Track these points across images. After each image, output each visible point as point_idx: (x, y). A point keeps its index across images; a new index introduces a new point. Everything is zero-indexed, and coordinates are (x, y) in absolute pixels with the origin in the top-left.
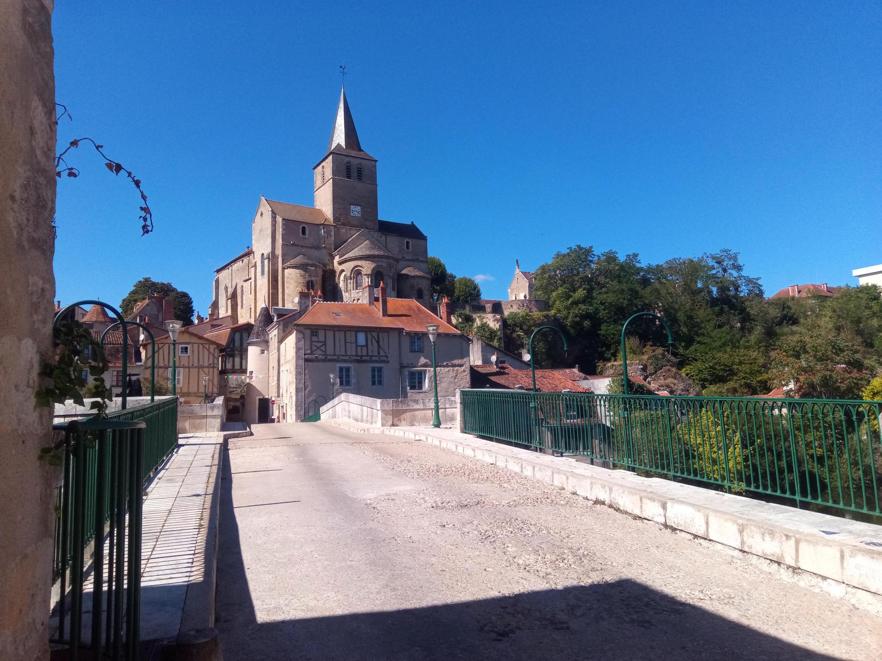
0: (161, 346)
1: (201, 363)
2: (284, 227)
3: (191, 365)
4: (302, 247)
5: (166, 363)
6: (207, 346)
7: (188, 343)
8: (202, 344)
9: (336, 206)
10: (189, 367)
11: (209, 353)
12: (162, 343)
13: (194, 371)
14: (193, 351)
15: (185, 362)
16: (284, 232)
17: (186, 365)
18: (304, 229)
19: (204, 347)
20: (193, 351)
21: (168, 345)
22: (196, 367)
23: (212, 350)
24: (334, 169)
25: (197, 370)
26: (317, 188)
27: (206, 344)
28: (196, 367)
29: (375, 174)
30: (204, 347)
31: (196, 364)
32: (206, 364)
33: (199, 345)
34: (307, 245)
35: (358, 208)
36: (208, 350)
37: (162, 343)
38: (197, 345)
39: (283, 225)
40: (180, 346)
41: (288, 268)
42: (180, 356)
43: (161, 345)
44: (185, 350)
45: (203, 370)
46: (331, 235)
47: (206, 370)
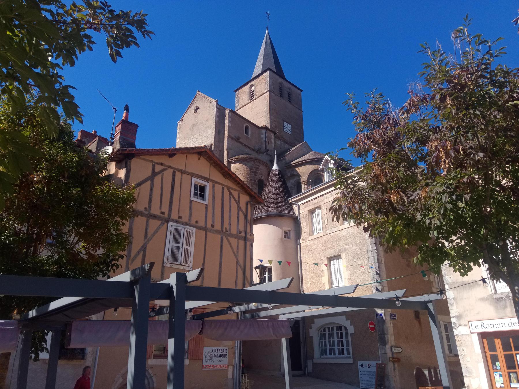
0: (158, 168)
1: (226, 225)
2: (231, 119)
3: (209, 226)
4: (246, 146)
5: (165, 209)
6: (235, 194)
7: (207, 180)
8: (229, 188)
9: (272, 117)
10: (205, 229)
11: (239, 208)
12: (161, 164)
13: (214, 239)
14: (214, 197)
15: (199, 216)
16: (230, 125)
17: (202, 224)
18: (247, 128)
19: (231, 194)
20: (214, 197)
21: (171, 171)
22: (218, 232)
23: (243, 205)
24: (271, 84)
25: (219, 236)
26: (240, 106)
27: (235, 190)
28: (218, 232)
29: (301, 101)
30: (231, 194)
31: (218, 227)
32: (234, 231)
33: (223, 189)
34: (250, 146)
35: (289, 126)
36: (238, 202)
37: (161, 164)
38: (221, 187)
39: (230, 117)
40: (195, 181)
41: (236, 162)
42: (191, 201)
43: (158, 168)
44: (200, 191)
45: (228, 241)
46: (271, 142)
47: (233, 241)
